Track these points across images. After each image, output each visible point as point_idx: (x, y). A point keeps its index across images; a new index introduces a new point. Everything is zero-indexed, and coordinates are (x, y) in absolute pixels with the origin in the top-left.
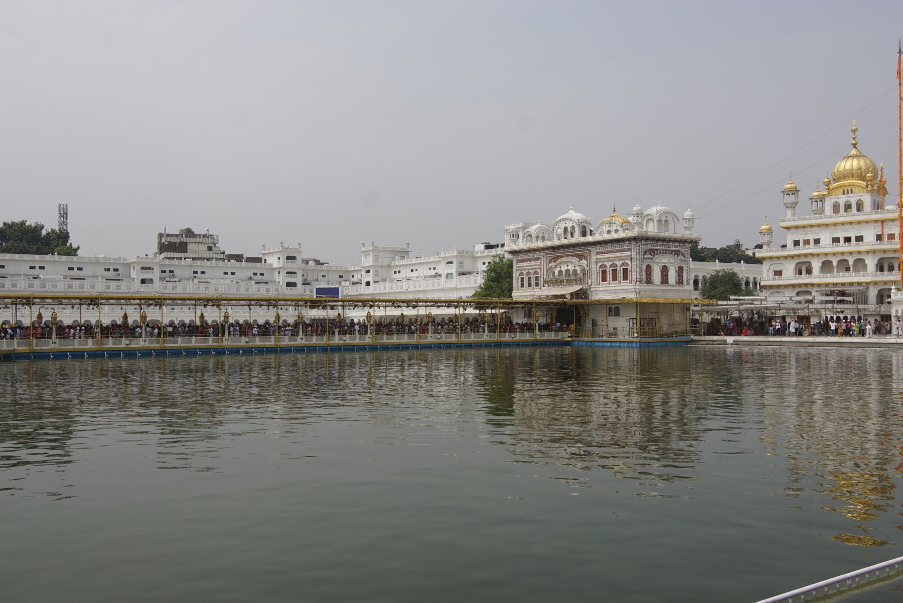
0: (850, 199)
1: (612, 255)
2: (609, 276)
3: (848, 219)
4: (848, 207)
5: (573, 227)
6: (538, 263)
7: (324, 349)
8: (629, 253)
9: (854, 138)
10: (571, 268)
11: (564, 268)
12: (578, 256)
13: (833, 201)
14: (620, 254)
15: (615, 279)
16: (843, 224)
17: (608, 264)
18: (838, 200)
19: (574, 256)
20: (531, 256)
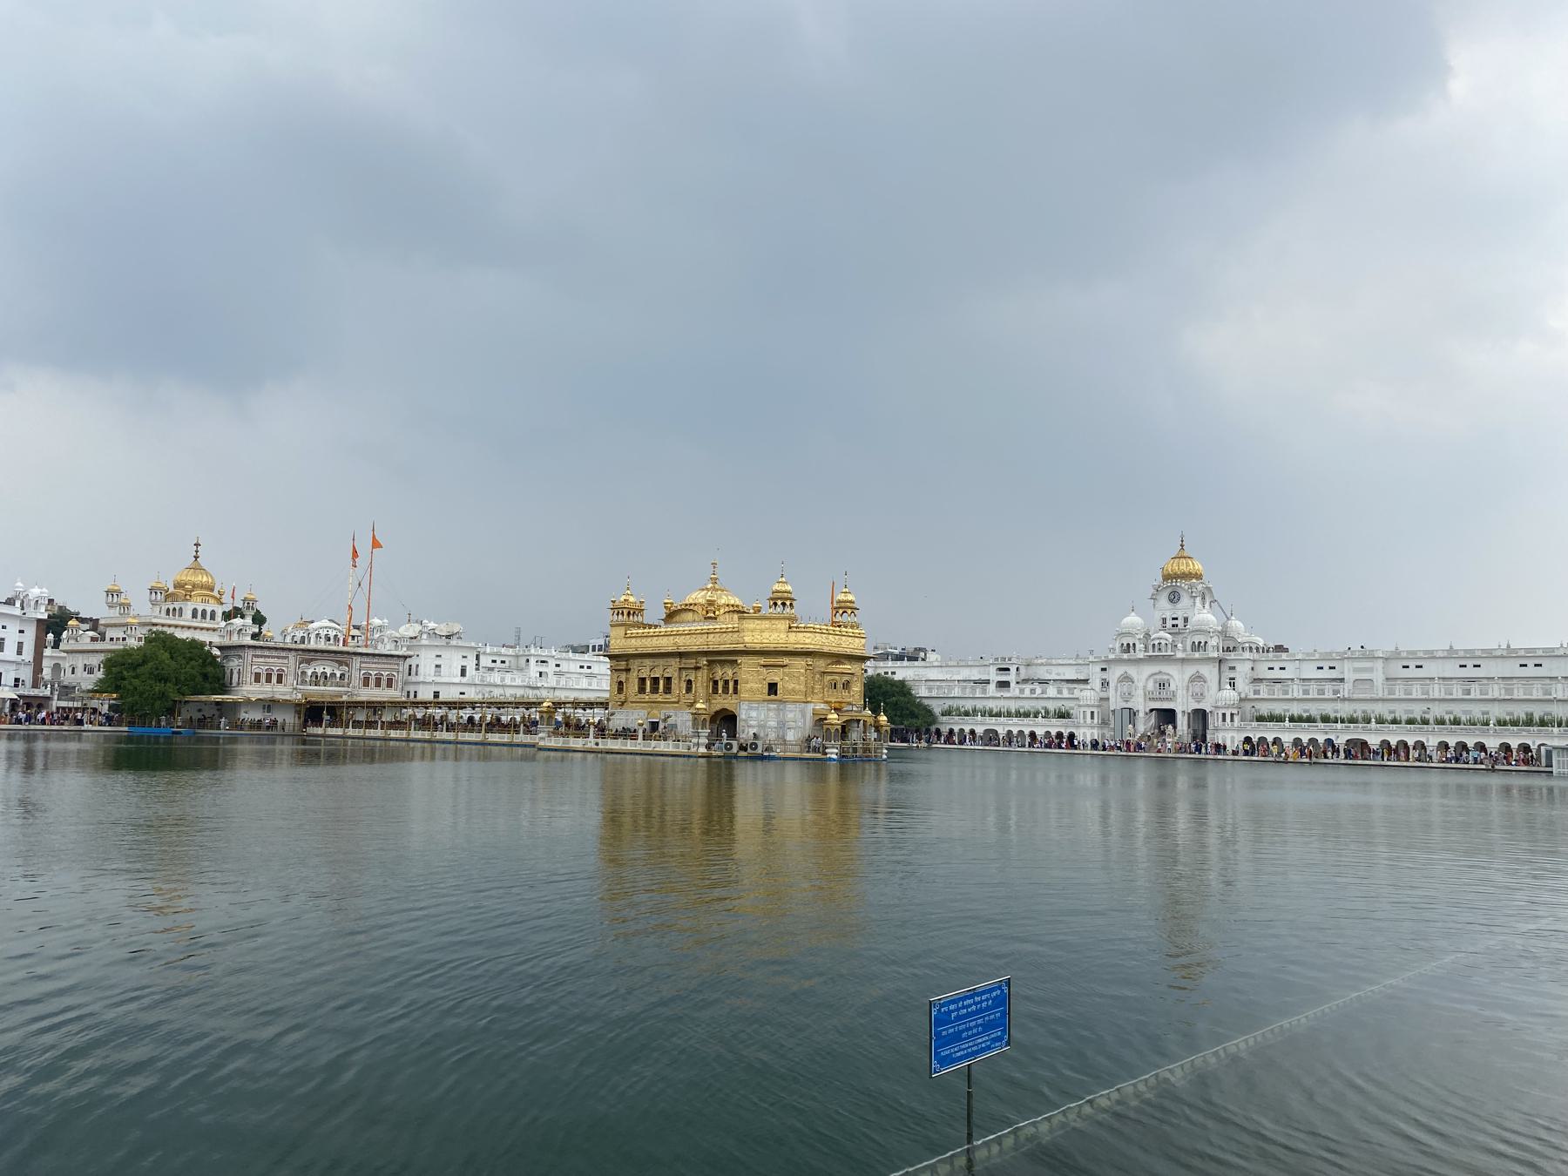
0: (207, 608)
1: (379, 666)
2: (372, 682)
3: (205, 625)
4: (204, 612)
5: (336, 636)
6: (286, 661)
7: (511, 745)
8: (396, 667)
9: (197, 552)
10: (328, 671)
11: (320, 670)
12: (337, 661)
13: (194, 607)
14: (386, 666)
15: (378, 684)
16: (202, 629)
17: (373, 673)
18: (197, 607)
19: (331, 660)
20: (274, 653)
